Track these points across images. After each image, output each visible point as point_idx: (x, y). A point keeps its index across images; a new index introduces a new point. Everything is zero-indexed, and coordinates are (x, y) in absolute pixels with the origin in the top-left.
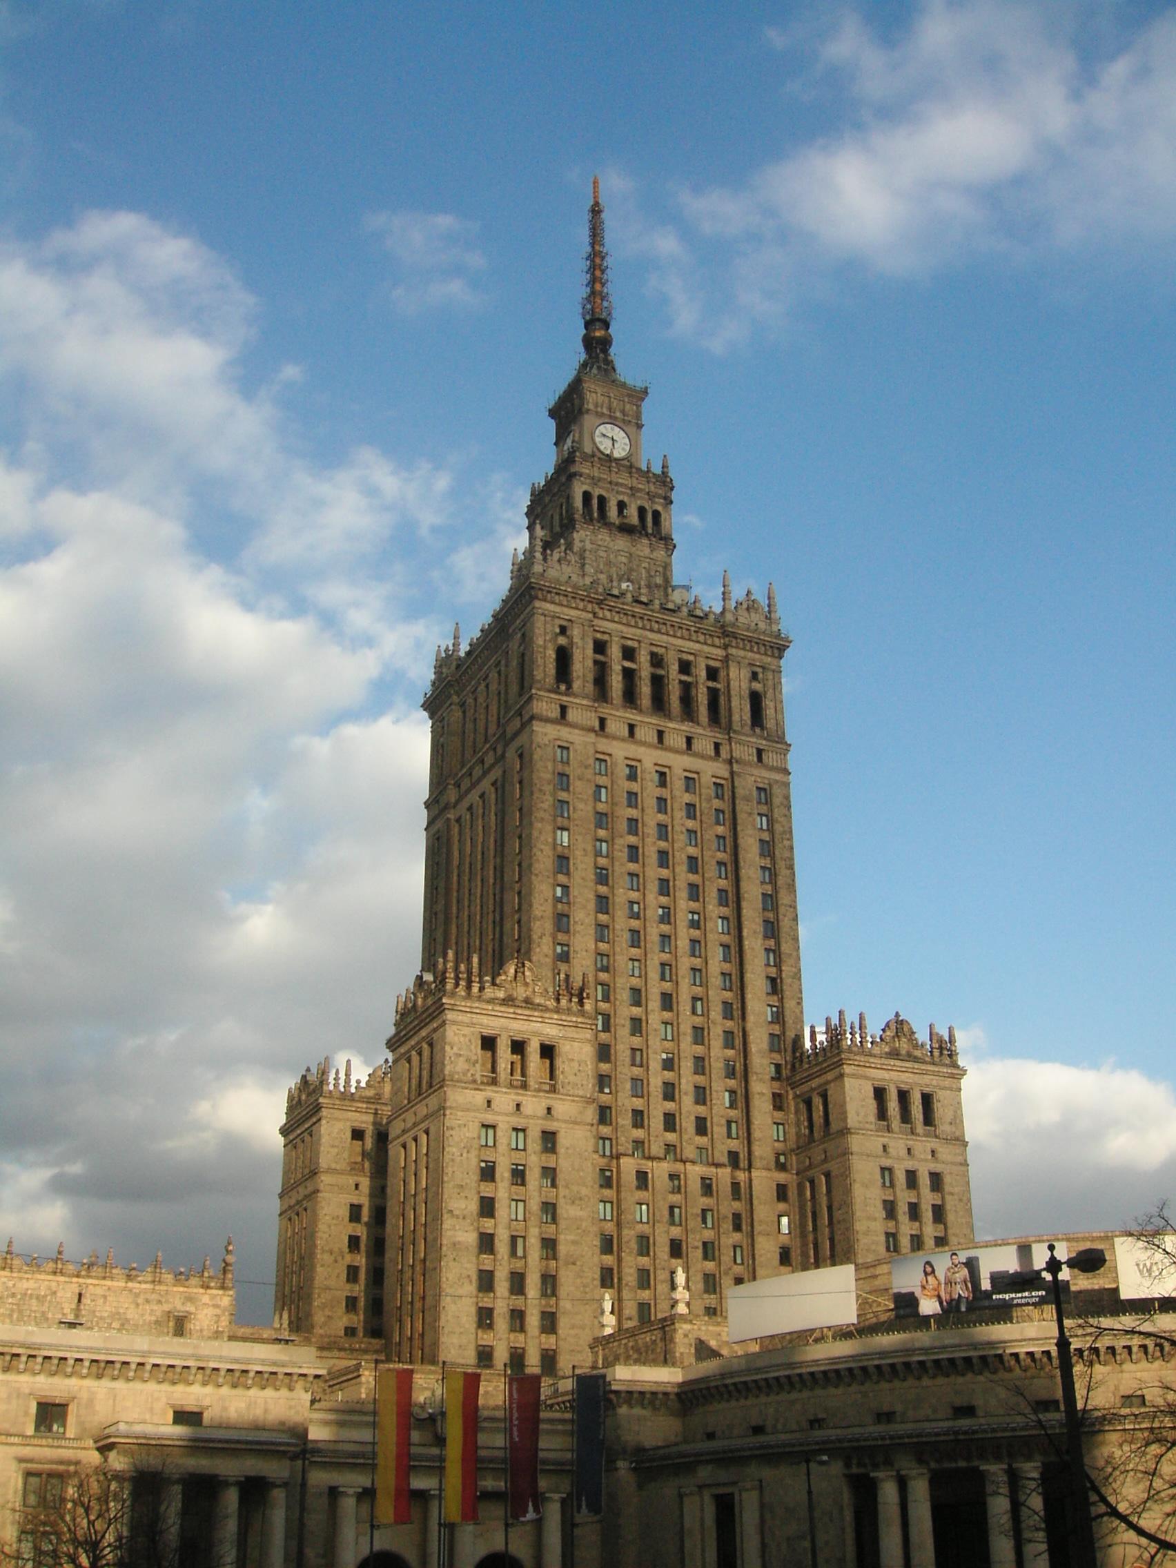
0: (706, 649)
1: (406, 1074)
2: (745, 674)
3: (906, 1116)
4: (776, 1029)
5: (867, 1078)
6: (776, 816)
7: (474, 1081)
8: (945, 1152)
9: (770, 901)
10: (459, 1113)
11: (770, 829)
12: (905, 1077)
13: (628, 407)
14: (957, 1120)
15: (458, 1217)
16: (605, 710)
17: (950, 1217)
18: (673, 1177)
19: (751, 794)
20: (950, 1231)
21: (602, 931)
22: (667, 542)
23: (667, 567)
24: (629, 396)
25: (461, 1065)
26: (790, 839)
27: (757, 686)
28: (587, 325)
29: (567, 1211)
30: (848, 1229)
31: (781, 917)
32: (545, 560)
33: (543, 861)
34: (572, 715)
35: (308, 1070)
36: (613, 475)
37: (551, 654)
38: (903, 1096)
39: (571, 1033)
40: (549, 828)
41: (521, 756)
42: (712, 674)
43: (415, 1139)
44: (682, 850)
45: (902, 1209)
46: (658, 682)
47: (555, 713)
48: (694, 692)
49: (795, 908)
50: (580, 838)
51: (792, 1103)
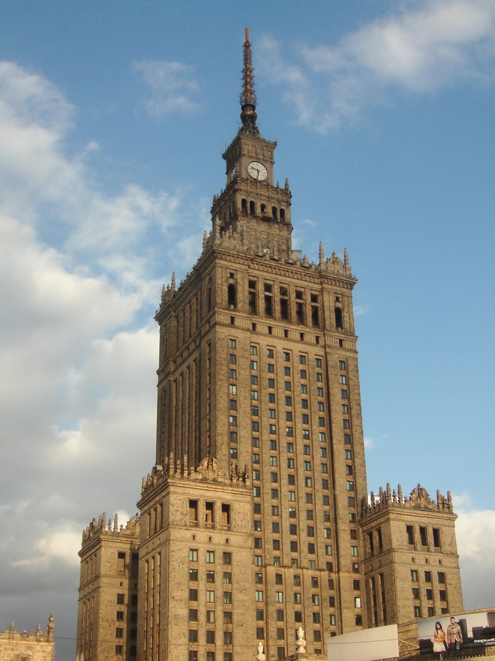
0: (310, 285)
1: (148, 522)
2: (332, 298)
3: (424, 542)
4: (352, 494)
5: (402, 521)
6: (350, 376)
7: (186, 525)
8: (447, 561)
9: (348, 423)
10: (178, 543)
11: (347, 384)
12: (423, 520)
13: (266, 152)
14: (453, 543)
15: (177, 601)
16: (255, 319)
17: (450, 597)
18: (296, 577)
19: (336, 364)
20: (450, 605)
21: (255, 441)
22: (288, 226)
23: (288, 240)
24: (267, 146)
25: (178, 516)
26: (358, 389)
27: (339, 305)
28: (243, 108)
29: (237, 596)
30: (393, 605)
31: (354, 432)
32: (221, 237)
33: (222, 403)
34: (237, 322)
35: (94, 520)
36: (258, 190)
37: (225, 289)
38: (423, 531)
39: (239, 497)
40: (226, 384)
41: (209, 345)
42: (314, 298)
43: (153, 558)
44: (299, 396)
45: (423, 593)
46: (284, 303)
47: (228, 321)
48: (304, 308)
49: (361, 427)
50: (243, 390)
51: (361, 535)
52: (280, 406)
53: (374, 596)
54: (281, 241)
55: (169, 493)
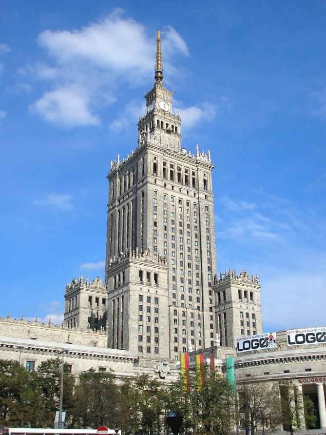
1: (114, 281)
5: (237, 287)
8: (256, 308)
17: (257, 326)
25: (134, 278)
27: (206, 178)
28: (157, 73)
29: (160, 320)
30: (231, 328)
33: (150, 223)
34: (158, 182)
37: (152, 165)
41: (143, 193)
42: (193, 174)
43: (118, 299)
44: (186, 223)
45: (245, 323)
46: (179, 174)
47: (154, 181)
51: (214, 294)
52: (177, 227)
53: (220, 324)
54: (176, 143)
55: (129, 266)
